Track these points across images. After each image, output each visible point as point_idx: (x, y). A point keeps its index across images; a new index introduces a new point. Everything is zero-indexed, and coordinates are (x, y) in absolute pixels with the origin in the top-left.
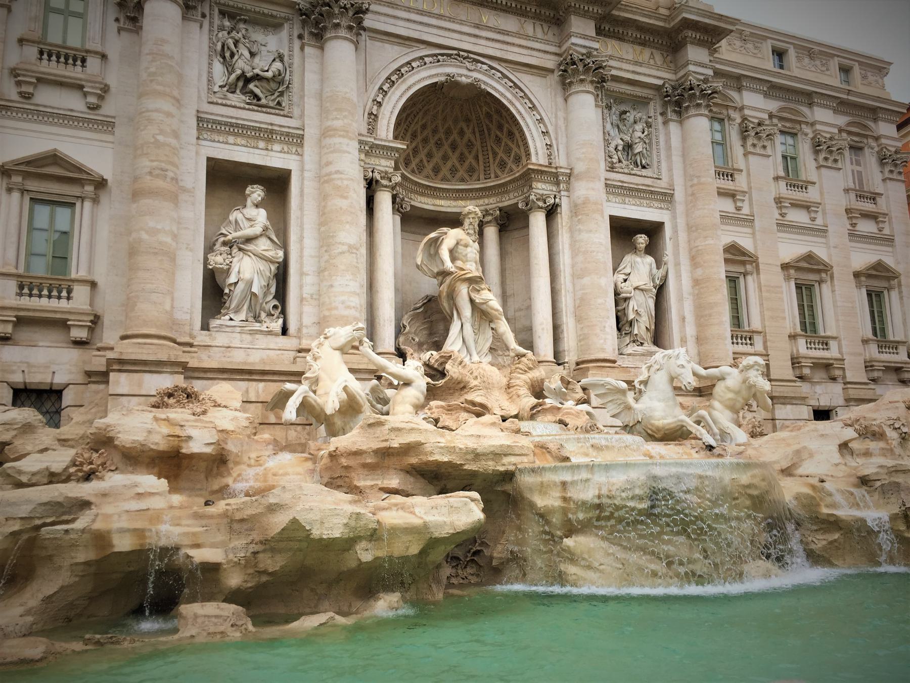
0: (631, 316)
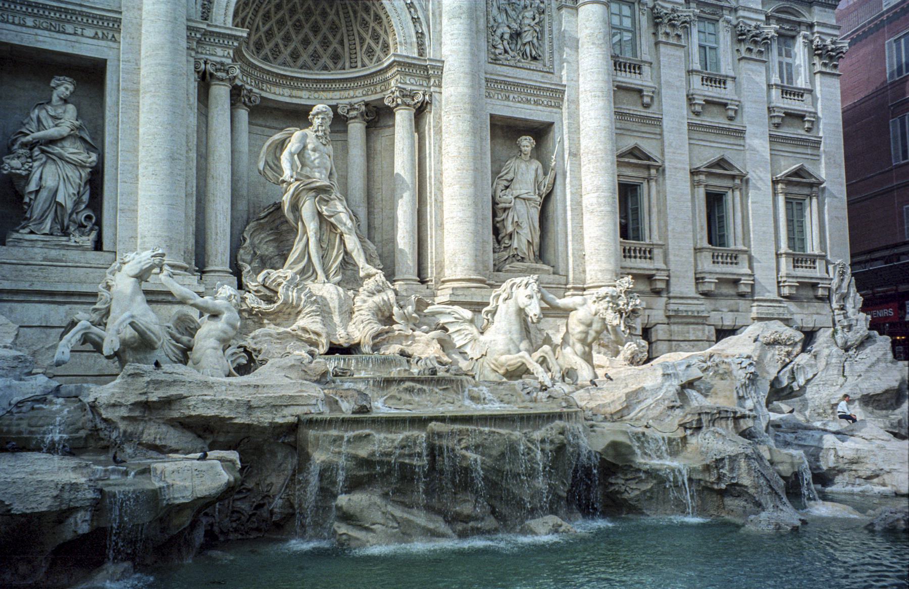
0: (510, 229)
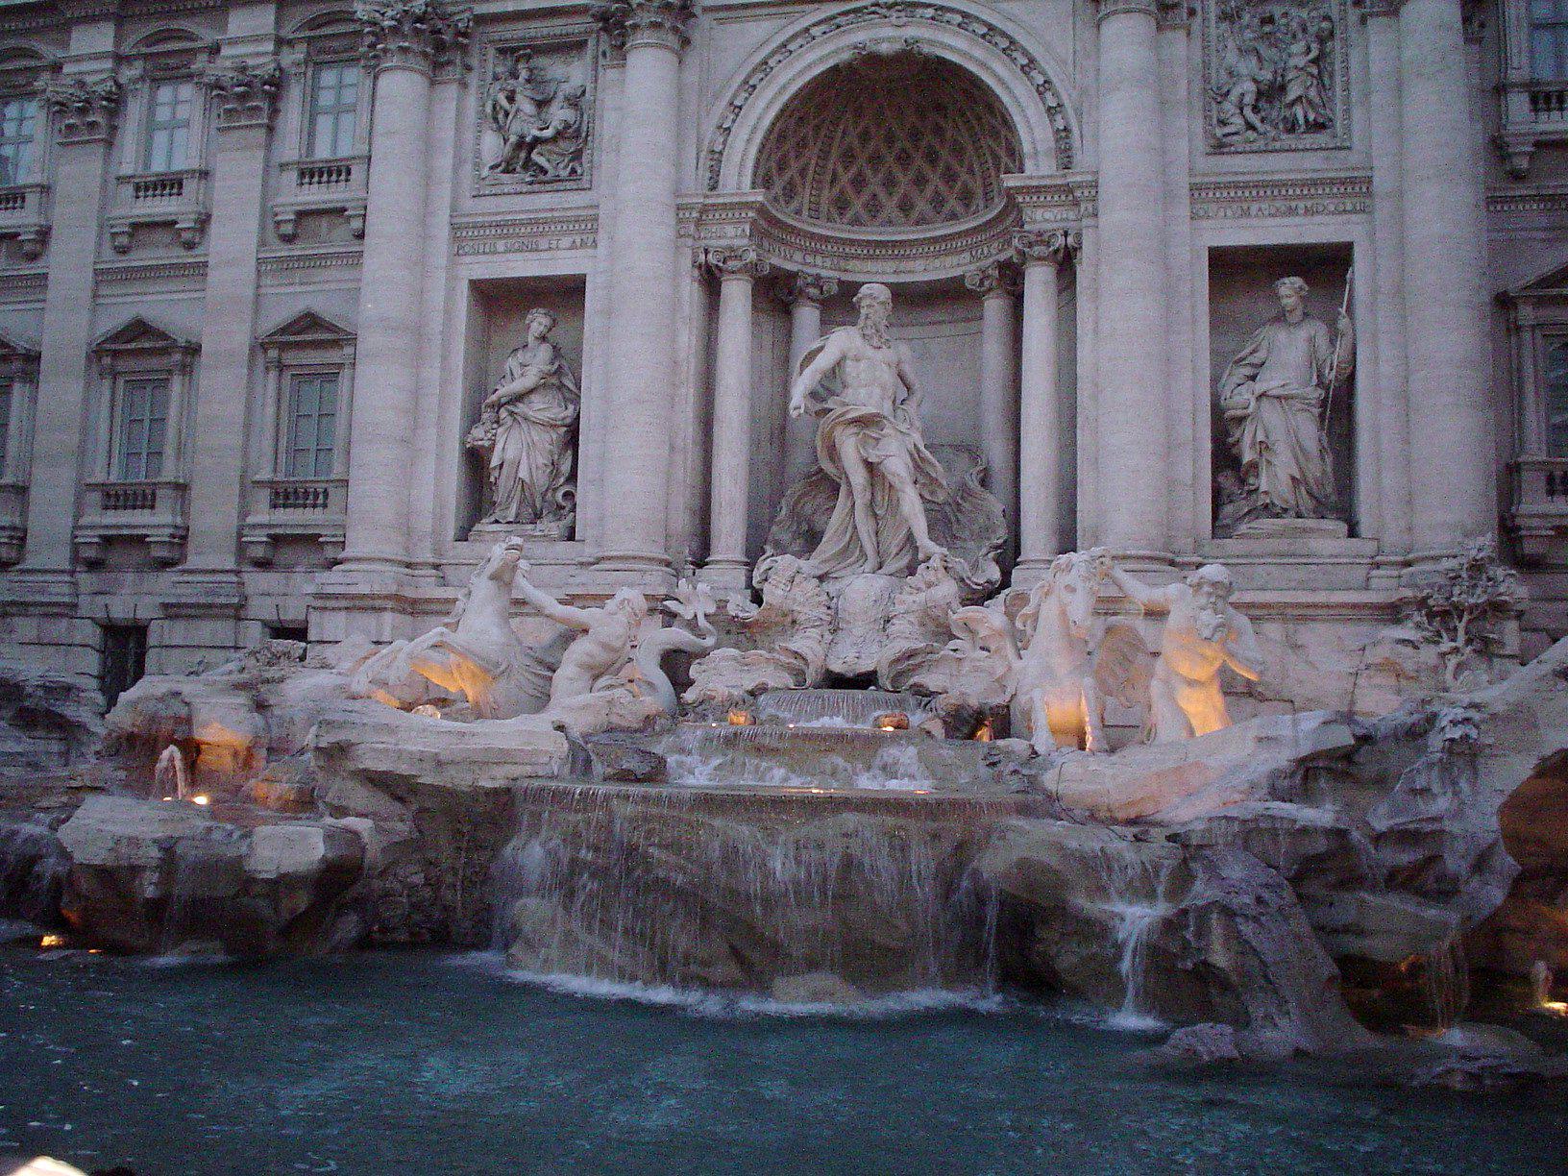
0: (1248, 456)
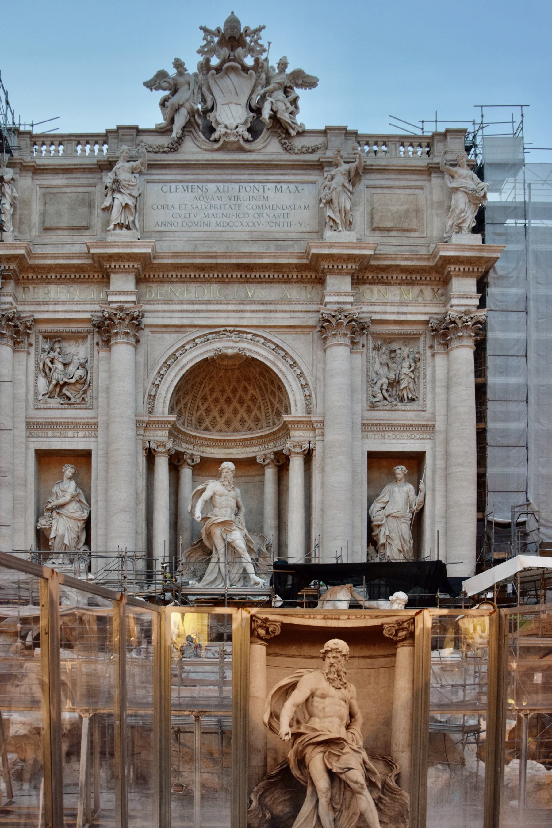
0: (382, 540)
